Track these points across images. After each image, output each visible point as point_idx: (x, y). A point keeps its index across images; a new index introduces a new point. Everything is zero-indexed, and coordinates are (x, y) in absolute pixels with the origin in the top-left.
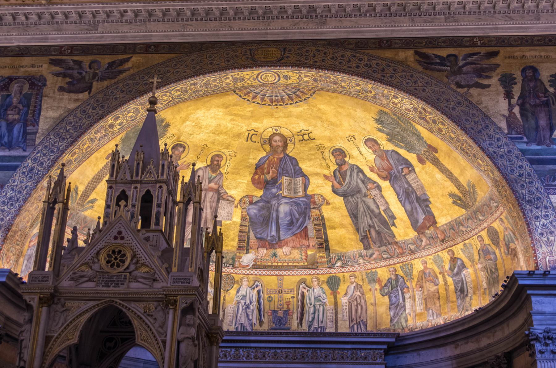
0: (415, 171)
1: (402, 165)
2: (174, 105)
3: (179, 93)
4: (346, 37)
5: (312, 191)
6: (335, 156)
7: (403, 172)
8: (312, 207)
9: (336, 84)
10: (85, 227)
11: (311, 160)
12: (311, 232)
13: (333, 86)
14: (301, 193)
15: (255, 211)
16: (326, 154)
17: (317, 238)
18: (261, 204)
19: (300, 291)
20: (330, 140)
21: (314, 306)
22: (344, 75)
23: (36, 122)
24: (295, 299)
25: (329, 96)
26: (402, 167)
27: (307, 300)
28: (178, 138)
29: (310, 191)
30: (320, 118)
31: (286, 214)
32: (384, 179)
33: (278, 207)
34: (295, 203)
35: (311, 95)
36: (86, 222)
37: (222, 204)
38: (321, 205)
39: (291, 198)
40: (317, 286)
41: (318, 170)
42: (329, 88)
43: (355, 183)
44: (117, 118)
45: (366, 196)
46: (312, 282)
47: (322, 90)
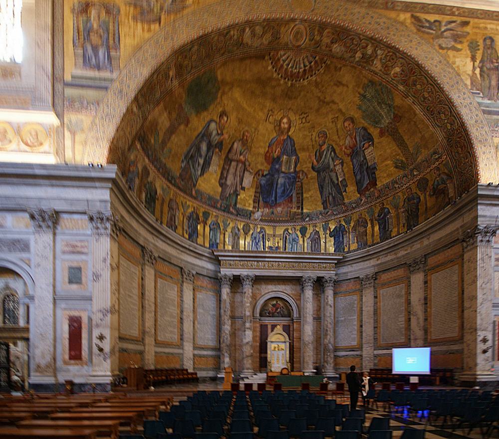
0: (373, 144)
1: (365, 140)
7: (363, 147)
8: (297, 180)
14: (292, 170)
15: (264, 182)
18: (268, 177)
23: (117, 47)
26: (364, 142)
29: (297, 169)
31: (281, 185)
32: (348, 155)
33: (278, 180)
37: (247, 174)
39: (286, 173)
43: (327, 161)
45: (332, 171)
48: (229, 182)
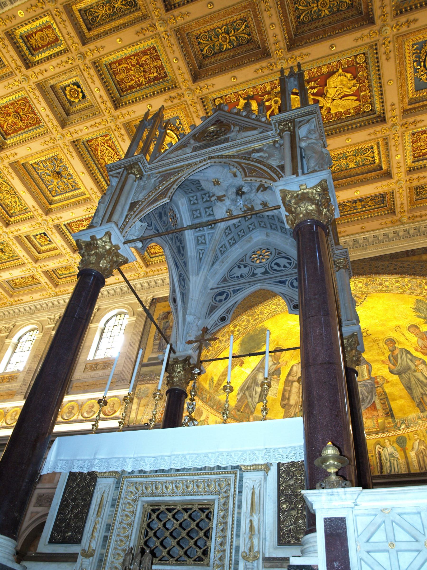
2: (273, 316)
3: (274, 307)
4: (382, 254)
5: (375, 374)
6: (387, 345)
8: (376, 386)
9: (381, 285)
10: (220, 407)
11: (370, 351)
12: (379, 406)
13: (380, 287)
14: (367, 377)
16: (381, 344)
17: (383, 409)
19: (377, 451)
20: (382, 333)
21: (390, 461)
22: (386, 275)
24: (374, 458)
25: (377, 297)
27: (383, 457)
28: (277, 343)
30: (372, 317)
34: (363, 384)
35: (365, 299)
36: (220, 404)
38: (383, 384)
40: (390, 446)
41: (377, 358)
42: (377, 289)
44: (235, 326)
46: (385, 443)
47: (372, 292)
48: (292, 402)
